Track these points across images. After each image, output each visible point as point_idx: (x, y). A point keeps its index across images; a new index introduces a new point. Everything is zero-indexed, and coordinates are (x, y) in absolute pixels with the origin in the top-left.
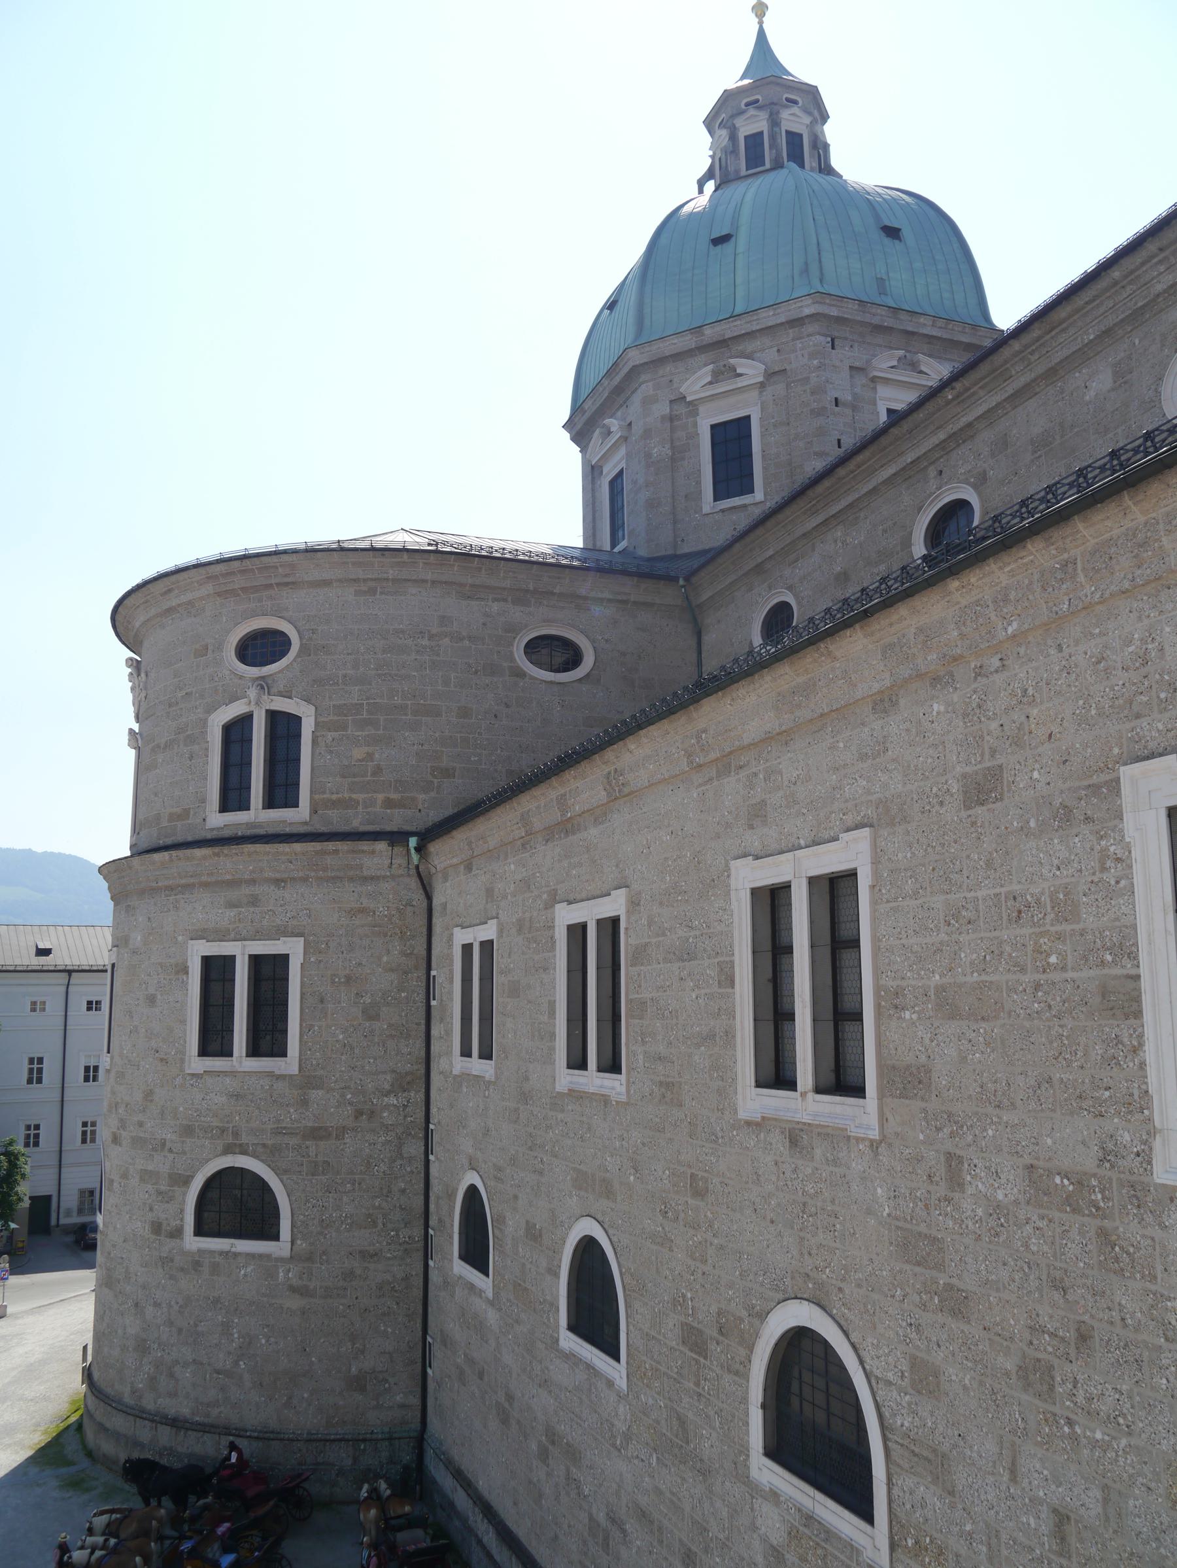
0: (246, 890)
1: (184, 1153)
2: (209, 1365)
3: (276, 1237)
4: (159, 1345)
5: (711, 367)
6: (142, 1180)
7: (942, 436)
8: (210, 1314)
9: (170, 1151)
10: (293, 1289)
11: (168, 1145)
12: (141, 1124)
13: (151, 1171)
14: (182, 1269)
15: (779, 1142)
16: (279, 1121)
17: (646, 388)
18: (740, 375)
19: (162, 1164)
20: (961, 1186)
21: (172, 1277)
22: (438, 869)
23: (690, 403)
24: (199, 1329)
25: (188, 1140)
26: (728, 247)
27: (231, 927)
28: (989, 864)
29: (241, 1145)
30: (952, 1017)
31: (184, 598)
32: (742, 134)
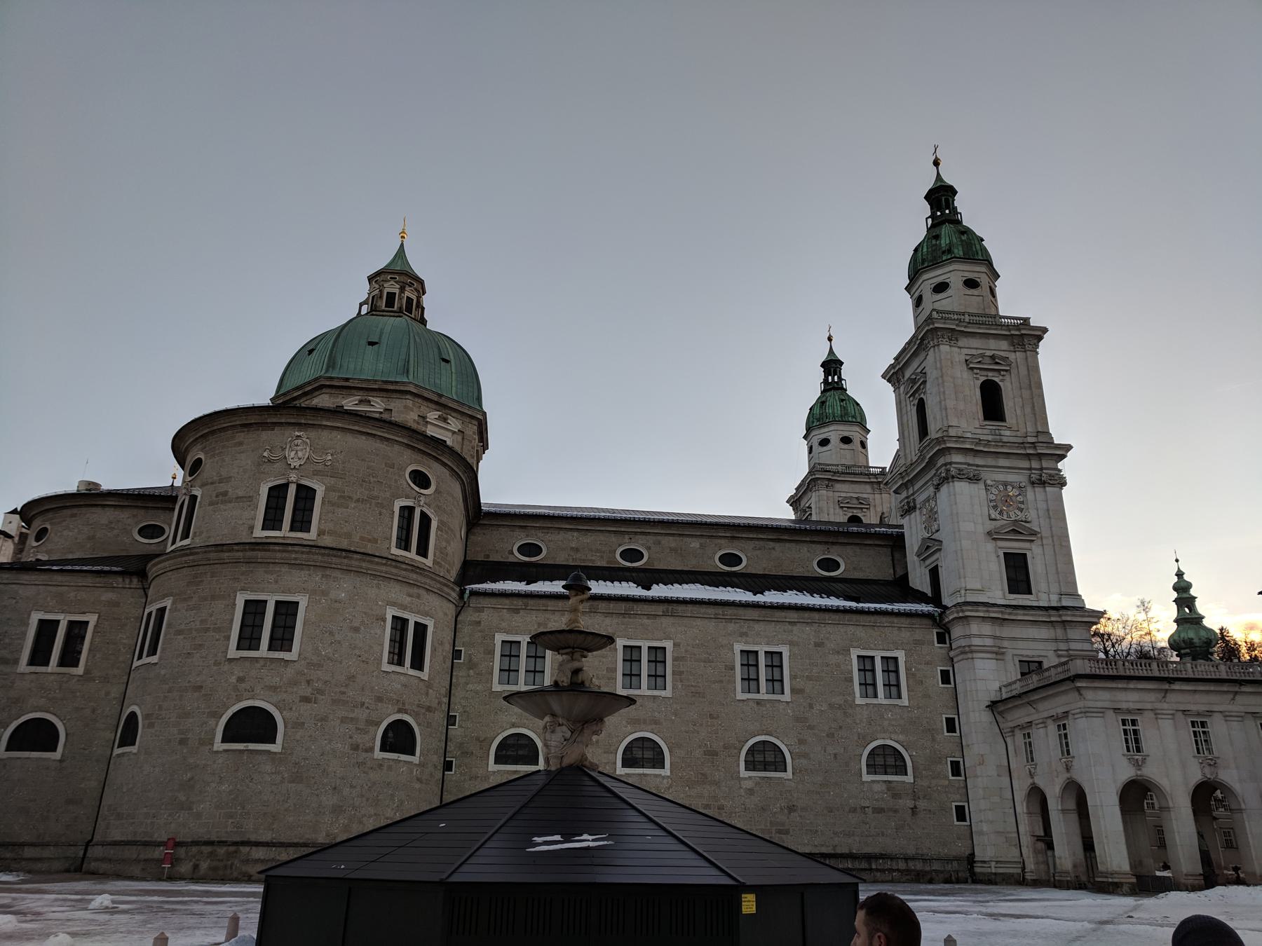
0: (416, 590)
1: (377, 710)
2: (383, 815)
3: (413, 754)
4: (353, 808)
5: (441, 413)
6: (342, 722)
7: (639, 530)
8: (385, 790)
9: (368, 708)
10: (418, 779)
11: (366, 705)
12: (344, 693)
13: (351, 718)
14: (372, 768)
15: (751, 703)
16: (419, 701)
17: (410, 403)
18: (448, 423)
19: (361, 714)
20: (813, 708)
21: (364, 773)
22: (471, 605)
23: (427, 422)
24: (379, 798)
25: (379, 704)
26: (448, 366)
27: (409, 605)
28: (821, 657)
29: (405, 709)
30: (810, 680)
31: (386, 435)
32: (407, 294)
